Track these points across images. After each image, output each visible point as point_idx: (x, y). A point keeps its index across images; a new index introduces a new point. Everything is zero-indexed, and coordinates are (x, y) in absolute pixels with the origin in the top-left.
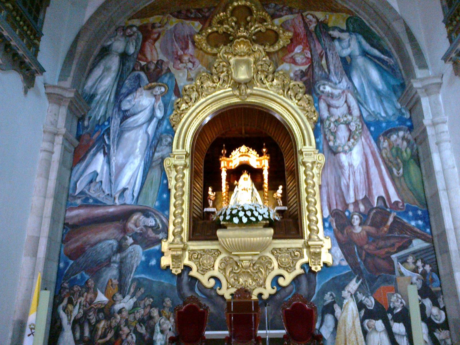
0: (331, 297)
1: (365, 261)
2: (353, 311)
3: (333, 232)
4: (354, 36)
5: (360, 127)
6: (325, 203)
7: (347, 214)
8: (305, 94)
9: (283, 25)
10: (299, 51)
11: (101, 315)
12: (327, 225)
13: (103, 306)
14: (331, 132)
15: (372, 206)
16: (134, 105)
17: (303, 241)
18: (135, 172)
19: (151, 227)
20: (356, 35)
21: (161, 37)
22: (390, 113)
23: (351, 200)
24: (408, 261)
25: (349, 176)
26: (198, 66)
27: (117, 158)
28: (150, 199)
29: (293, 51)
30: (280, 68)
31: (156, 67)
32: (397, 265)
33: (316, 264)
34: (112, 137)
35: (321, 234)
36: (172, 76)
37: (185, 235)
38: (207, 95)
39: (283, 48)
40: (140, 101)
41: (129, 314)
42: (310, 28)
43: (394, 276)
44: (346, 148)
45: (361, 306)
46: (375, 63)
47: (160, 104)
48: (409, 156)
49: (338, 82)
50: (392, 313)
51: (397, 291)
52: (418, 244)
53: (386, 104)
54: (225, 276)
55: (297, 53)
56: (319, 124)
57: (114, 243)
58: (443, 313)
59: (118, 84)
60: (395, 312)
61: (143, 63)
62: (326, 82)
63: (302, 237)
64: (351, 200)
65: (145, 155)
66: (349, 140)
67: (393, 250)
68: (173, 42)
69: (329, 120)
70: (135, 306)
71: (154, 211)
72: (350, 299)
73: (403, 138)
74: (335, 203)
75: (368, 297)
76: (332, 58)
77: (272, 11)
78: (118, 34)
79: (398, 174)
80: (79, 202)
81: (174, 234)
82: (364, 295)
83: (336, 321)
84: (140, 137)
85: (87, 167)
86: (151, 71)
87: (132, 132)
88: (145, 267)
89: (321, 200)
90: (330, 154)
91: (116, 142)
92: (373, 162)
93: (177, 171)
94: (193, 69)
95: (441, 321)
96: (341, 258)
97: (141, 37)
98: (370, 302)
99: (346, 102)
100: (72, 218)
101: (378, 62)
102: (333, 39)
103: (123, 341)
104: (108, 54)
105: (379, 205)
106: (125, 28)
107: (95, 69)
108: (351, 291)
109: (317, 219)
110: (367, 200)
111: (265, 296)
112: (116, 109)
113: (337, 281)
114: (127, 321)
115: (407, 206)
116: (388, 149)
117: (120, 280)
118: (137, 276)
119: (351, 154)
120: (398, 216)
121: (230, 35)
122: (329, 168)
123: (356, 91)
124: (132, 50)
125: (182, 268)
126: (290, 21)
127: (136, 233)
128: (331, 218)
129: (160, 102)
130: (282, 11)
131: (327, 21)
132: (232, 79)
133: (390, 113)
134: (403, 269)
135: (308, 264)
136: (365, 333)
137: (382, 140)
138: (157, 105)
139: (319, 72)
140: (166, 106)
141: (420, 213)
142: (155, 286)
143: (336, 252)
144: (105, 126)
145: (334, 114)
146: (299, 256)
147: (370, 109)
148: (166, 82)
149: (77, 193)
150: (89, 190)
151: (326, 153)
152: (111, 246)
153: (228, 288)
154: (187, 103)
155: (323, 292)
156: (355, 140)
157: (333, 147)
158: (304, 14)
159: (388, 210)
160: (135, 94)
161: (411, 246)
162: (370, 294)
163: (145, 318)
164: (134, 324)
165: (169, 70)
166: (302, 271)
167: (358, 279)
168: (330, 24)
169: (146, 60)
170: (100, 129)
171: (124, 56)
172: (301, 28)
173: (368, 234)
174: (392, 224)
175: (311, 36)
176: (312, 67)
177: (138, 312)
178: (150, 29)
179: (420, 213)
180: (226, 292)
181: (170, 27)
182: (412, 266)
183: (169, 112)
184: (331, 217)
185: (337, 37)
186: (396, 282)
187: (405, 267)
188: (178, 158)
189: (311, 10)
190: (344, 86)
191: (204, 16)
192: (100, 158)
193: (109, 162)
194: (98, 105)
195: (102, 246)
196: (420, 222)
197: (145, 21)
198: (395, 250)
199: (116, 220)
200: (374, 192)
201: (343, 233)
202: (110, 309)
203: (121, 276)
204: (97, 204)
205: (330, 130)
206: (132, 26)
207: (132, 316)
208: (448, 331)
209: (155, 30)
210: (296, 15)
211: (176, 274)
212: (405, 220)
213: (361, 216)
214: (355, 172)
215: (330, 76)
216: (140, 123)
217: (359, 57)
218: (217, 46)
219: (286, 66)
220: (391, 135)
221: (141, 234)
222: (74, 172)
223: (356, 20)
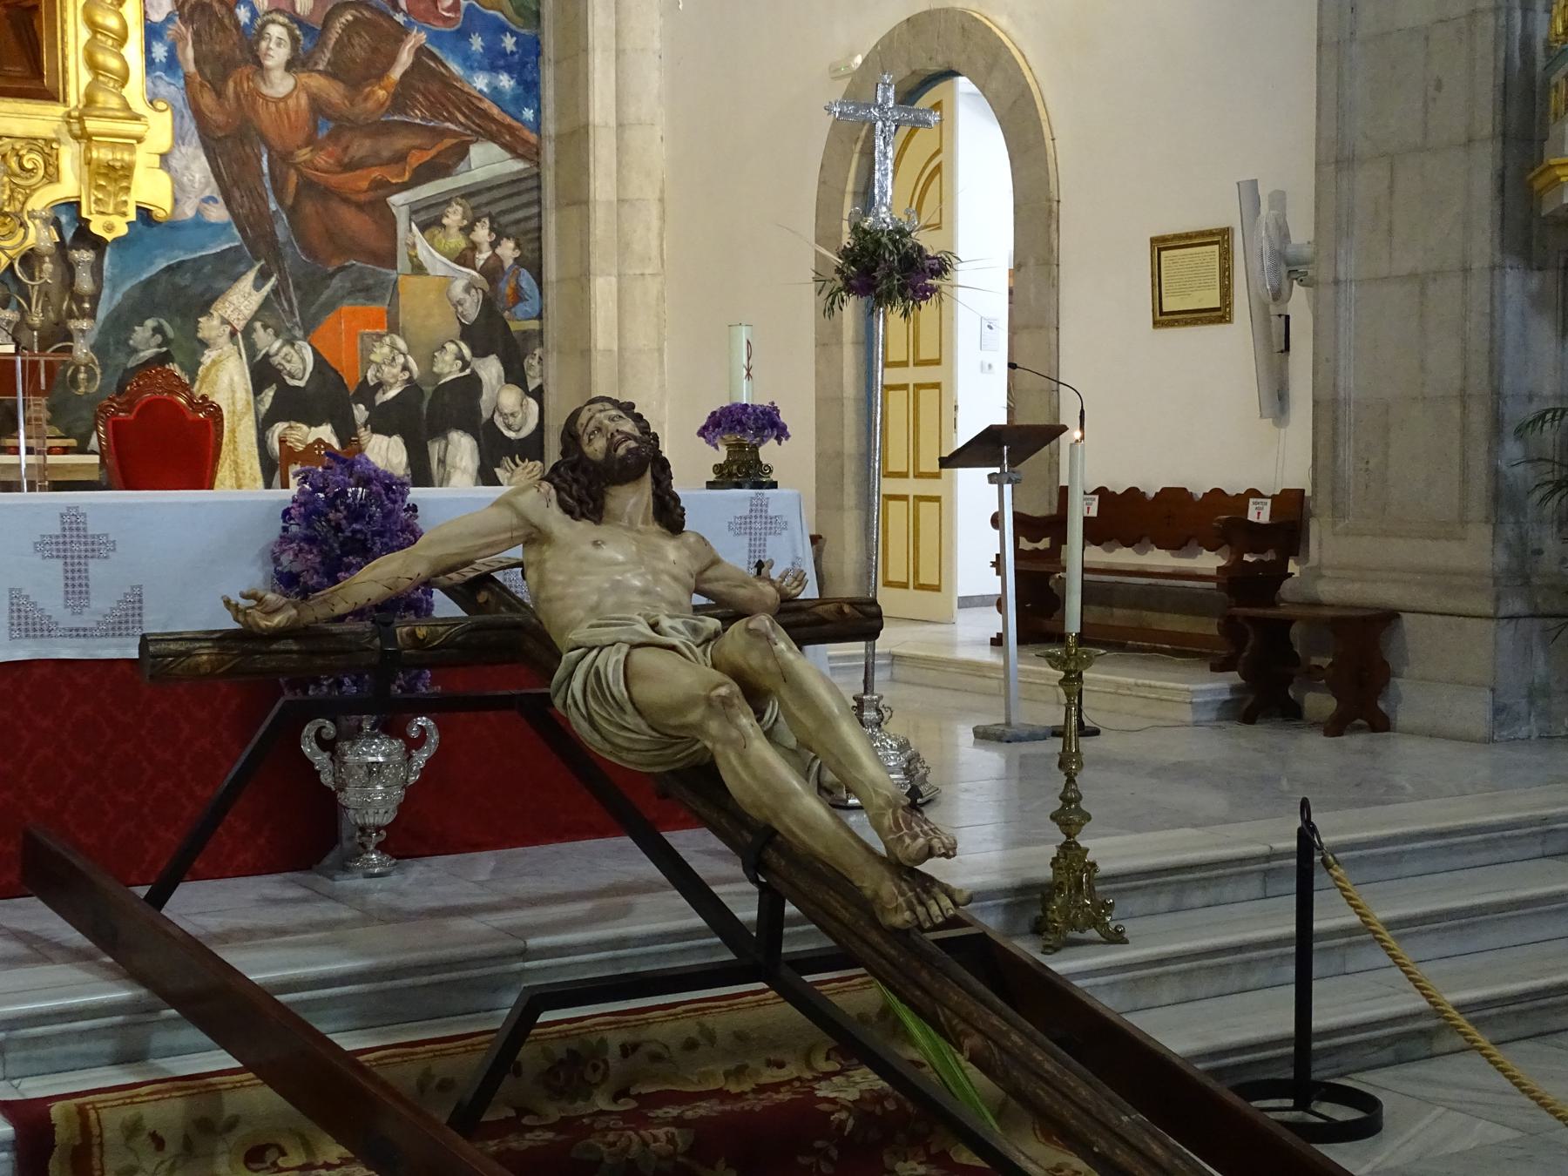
1: (292, 212)
2: (233, 392)
3: (182, 82)
12: (160, 52)
17: (58, 110)
24: (445, 221)
32: (409, 234)
33: (111, 209)
45: (263, 373)
50: (370, 406)
51: (394, 328)
58: (533, 406)
60: (383, 397)
67: (398, 176)
72: (229, 348)
75: (291, 342)
82: (277, 335)
95: (524, 433)
96: (207, 193)
98: (298, 362)
108: (233, 318)
109: (125, 27)
113: (184, 280)
120: (435, 50)
128: (178, 26)
135: (73, 206)
141: (509, 43)
143: (187, 168)
146: (41, 172)
159: (400, 18)
161: (462, 166)
162: (298, 333)
167: (263, 276)
173: (318, 107)
174: (405, 74)
179: (509, 43)
184: (177, 19)
186: (395, 293)
196: (506, 82)
198: (406, 178)
201: (220, 94)
208: (539, 463)
212: (455, 68)
213: (298, 32)
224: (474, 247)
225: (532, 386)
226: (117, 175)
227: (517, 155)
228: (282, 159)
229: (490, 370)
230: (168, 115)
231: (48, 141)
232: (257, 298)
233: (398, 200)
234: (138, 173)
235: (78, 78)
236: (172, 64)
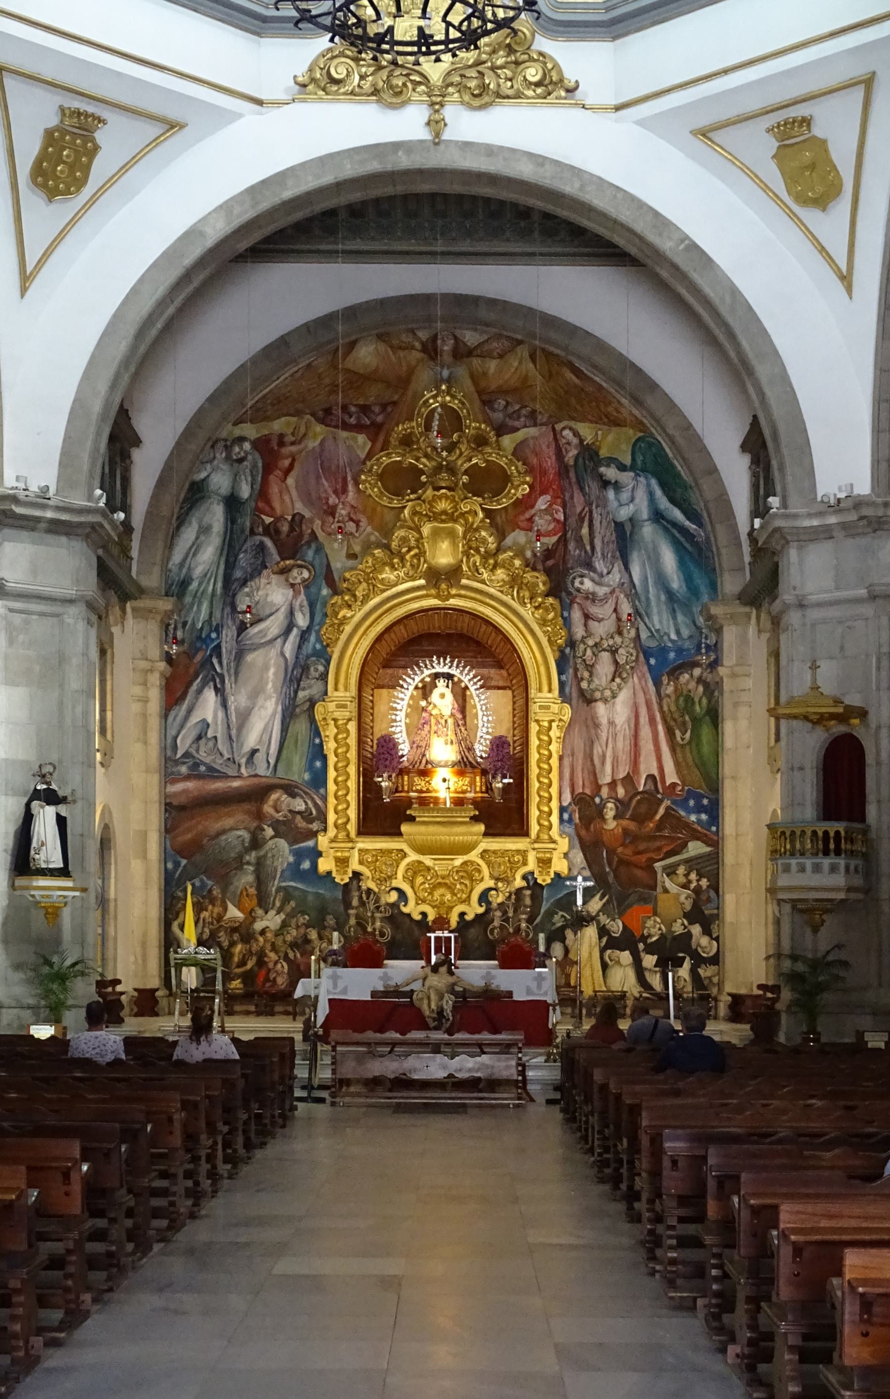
0: (563, 919)
4: (642, 479)
5: (634, 658)
6: (566, 782)
7: (597, 800)
8: (547, 595)
9: (518, 452)
10: (543, 507)
11: (236, 937)
12: (566, 816)
13: (237, 924)
14: (586, 665)
15: (637, 789)
16: (257, 603)
17: (528, 840)
18: (268, 723)
19: (299, 813)
20: (646, 478)
21: (297, 465)
22: (685, 633)
23: (606, 778)
25: (607, 740)
26: (365, 530)
27: (238, 700)
28: (295, 768)
29: (533, 506)
30: (509, 541)
31: (292, 529)
34: (225, 662)
35: (555, 832)
36: (320, 549)
37: (352, 827)
38: (383, 591)
39: (518, 503)
40: (267, 595)
41: (276, 935)
42: (566, 459)
43: (655, 893)
44: (608, 693)
45: (603, 931)
46: (673, 536)
47: (302, 602)
48: (703, 712)
49: (605, 571)
50: (645, 944)
51: (655, 914)
52: (695, 848)
53: (680, 618)
54: (412, 887)
55: (541, 510)
56: (568, 650)
57: (246, 835)
58: (715, 943)
59: (227, 562)
60: (649, 941)
61: (268, 520)
62: (587, 572)
63: (526, 834)
64: (606, 778)
65: (283, 694)
66: (613, 680)
68: (318, 478)
69: (585, 644)
70: (284, 925)
71: (303, 788)
73: (700, 680)
74: (581, 783)
76: (601, 522)
77: (498, 416)
78: (218, 455)
79: (683, 739)
80: (184, 769)
81: (336, 826)
83: (567, 951)
84: (273, 661)
85: (189, 711)
86: (283, 536)
87: (256, 653)
88: (295, 872)
89: (561, 778)
90: (581, 700)
91: (232, 671)
92: (647, 719)
93: (337, 727)
94: (357, 535)
95: (711, 954)
97: (260, 465)
98: (617, 927)
99: (615, 610)
100: (175, 795)
101: (678, 535)
102: (605, 484)
103: (269, 970)
104: (203, 498)
105: (648, 787)
106: (229, 443)
107: (183, 529)
110: (629, 780)
111: (469, 917)
112: (228, 610)
114: (273, 945)
115: (689, 790)
116: (673, 698)
117: (258, 889)
118: (284, 884)
119: (614, 703)
121: (422, 472)
122: (577, 725)
123: (633, 591)
124: (245, 492)
125: (351, 875)
126: (531, 442)
127: (278, 821)
129: (302, 597)
130: (519, 417)
131: (598, 443)
132: (425, 561)
133: (685, 633)
134: (668, 884)
136: (605, 966)
137: (665, 681)
138: (298, 604)
139: (575, 551)
140: (312, 606)
141: (705, 802)
142: (310, 898)
144: (213, 640)
145: (593, 631)
147: (653, 626)
148: (311, 559)
149: (179, 756)
150: (197, 751)
151: (574, 701)
152: (240, 839)
153: (417, 904)
154: (349, 607)
155: (550, 914)
156: (623, 679)
157: (586, 690)
158: (558, 427)
159: (659, 796)
160: (257, 580)
161: (685, 850)
162: (617, 916)
163: (299, 941)
164: (283, 949)
165: (313, 534)
166: (524, 884)
168: (604, 453)
169: (271, 513)
170: (204, 647)
171: (232, 503)
172: (549, 458)
173: (626, 832)
174: (662, 816)
175: (568, 477)
176: (563, 541)
177: (288, 933)
178: (276, 448)
179: (705, 802)
180: (412, 909)
181: (312, 444)
182: (682, 880)
183: (317, 619)
185: (613, 481)
187: (671, 880)
188: (338, 706)
189: (573, 419)
190: (614, 581)
191: (373, 424)
192: (210, 697)
193: (224, 705)
194: (197, 600)
195: (226, 840)
196: (704, 817)
197: (265, 430)
199: (243, 801)
200: (642, 767)
201: (587, 829)
202: (248, 929)
203: (261, 883)
204: (213, 774)
205: (584, 660)
206: (241, 439)
207: (281, 938)
209: (286, 450)
210: (544, 428)
211: (342, 883)
212: (683, 813)
214: (616, 734)
215: (594, 559)
216: (270, 637)
217: (647, 523)
218: (398, 493)
219: (517, 537)
220: (681, 673)
221: (284, 823)
222: (170, 718)
223: (650, 445)
224: (690, 882)
225: (714, 936)
226: (545, 863)
227: (708, 845)
228: (611, 852)
229: (696, 930)
230: (567, 840)
231: (525, 851)
232: (601, 904)
233: (658, 865)
234: (554, 861)
235: (534, 828)
236: (570, 820)
